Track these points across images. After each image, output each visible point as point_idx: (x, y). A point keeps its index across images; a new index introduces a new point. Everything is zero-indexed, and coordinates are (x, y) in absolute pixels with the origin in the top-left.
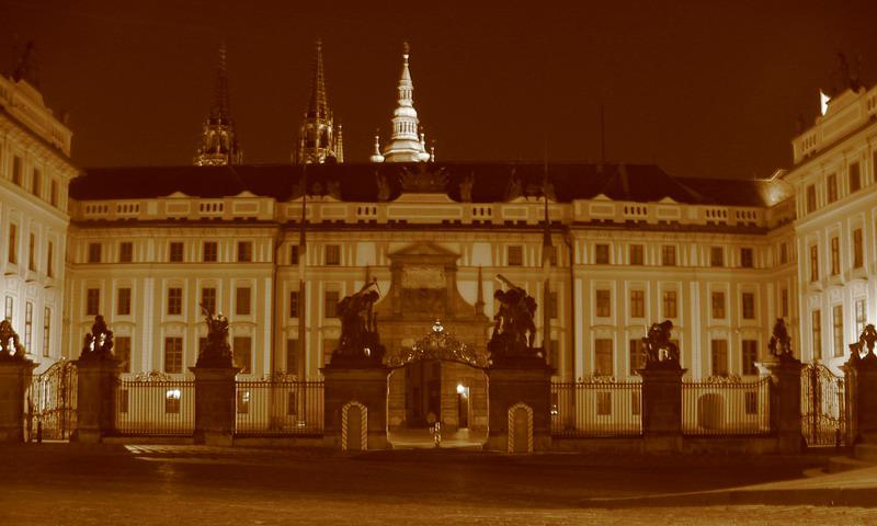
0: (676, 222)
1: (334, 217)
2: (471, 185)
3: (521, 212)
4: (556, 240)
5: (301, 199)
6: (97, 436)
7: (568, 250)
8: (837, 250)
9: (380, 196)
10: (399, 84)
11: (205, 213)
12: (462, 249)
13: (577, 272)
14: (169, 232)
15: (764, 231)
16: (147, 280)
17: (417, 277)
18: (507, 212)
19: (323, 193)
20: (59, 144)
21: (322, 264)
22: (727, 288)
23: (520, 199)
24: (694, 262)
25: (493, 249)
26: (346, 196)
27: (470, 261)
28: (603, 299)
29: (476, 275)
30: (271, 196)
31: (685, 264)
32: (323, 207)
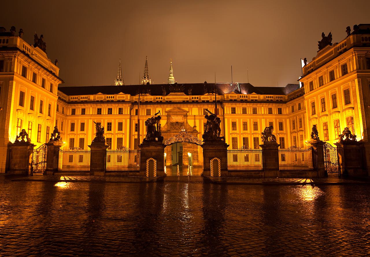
4: (219, 107)
5: (138, 95)
6: (52, 172)
7: (222, 110)
12: (189, 110)
13: (225, 116)
14: (97, 105)
15: (285, 102)
16: (90, 120)
17: (175, 119)
21: (145, 115)
22: (274, 121)
24: (263, 113)
25: (199, 110)
28: (234, 125)
30: (129, 94)
31: (260, 113)
32: (145, 97)
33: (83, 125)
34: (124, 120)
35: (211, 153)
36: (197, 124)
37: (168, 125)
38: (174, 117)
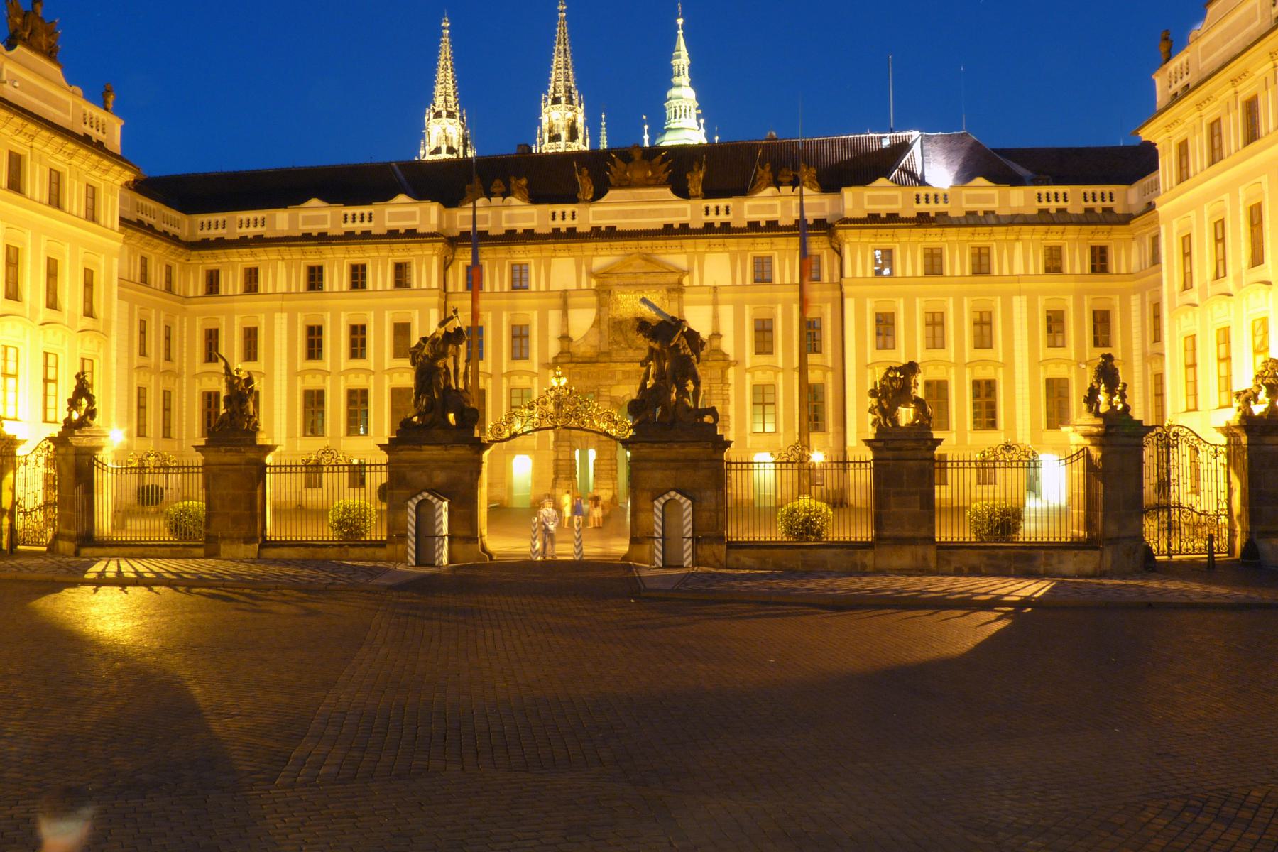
0: (993, 212)
1: (520, 226)
2: (701, 175)
3: (772, 208)
8: (1223, 240)
9: (580, 196)
10: (671, 58)
11: (349, 226)
13: (846, 289)
14: (304, 253)
15: (1126, 219)
16: (277, 315)
18: (753, 209)
19: (505, 195)
20: (96, 135)
21: (506, 289)
22: (1069, 305)
23: (770, 191)
24: (1019, 269)
26: (536, 197)
27: (701, 278)
29: (559, 301)
30: (433, 200)
31: (1006, 272)
32: (505, 212)
33: (250, 336)
34: (417, 311)
35: (658, 475)
36: (727, 328)
37: (600, 332)
38: (624, 296)
